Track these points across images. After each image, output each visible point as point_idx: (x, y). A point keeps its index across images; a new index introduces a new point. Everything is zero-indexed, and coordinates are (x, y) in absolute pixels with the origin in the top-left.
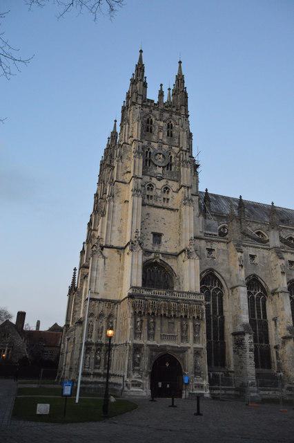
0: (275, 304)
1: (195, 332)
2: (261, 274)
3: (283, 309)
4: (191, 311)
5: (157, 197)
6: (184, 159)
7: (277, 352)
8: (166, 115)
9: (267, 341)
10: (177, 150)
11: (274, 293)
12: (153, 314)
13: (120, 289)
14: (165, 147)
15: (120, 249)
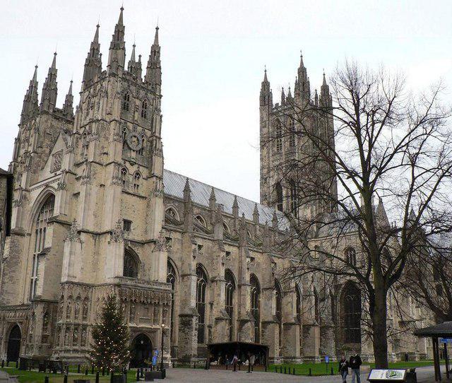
0: (213, 290)
1: (163, 316)
2: (205, 263)
3: (219, 295)
4: (163, 299)
5: (128, 181)
6: (157, 147)
7: (210, 332)
8: (142, 93)
9: (203, 321)
10: (149, 133)
11: (213, 281)
12: (135, 300)
13: (95, 274)
14: (139, 129)
15: (96, 235)
